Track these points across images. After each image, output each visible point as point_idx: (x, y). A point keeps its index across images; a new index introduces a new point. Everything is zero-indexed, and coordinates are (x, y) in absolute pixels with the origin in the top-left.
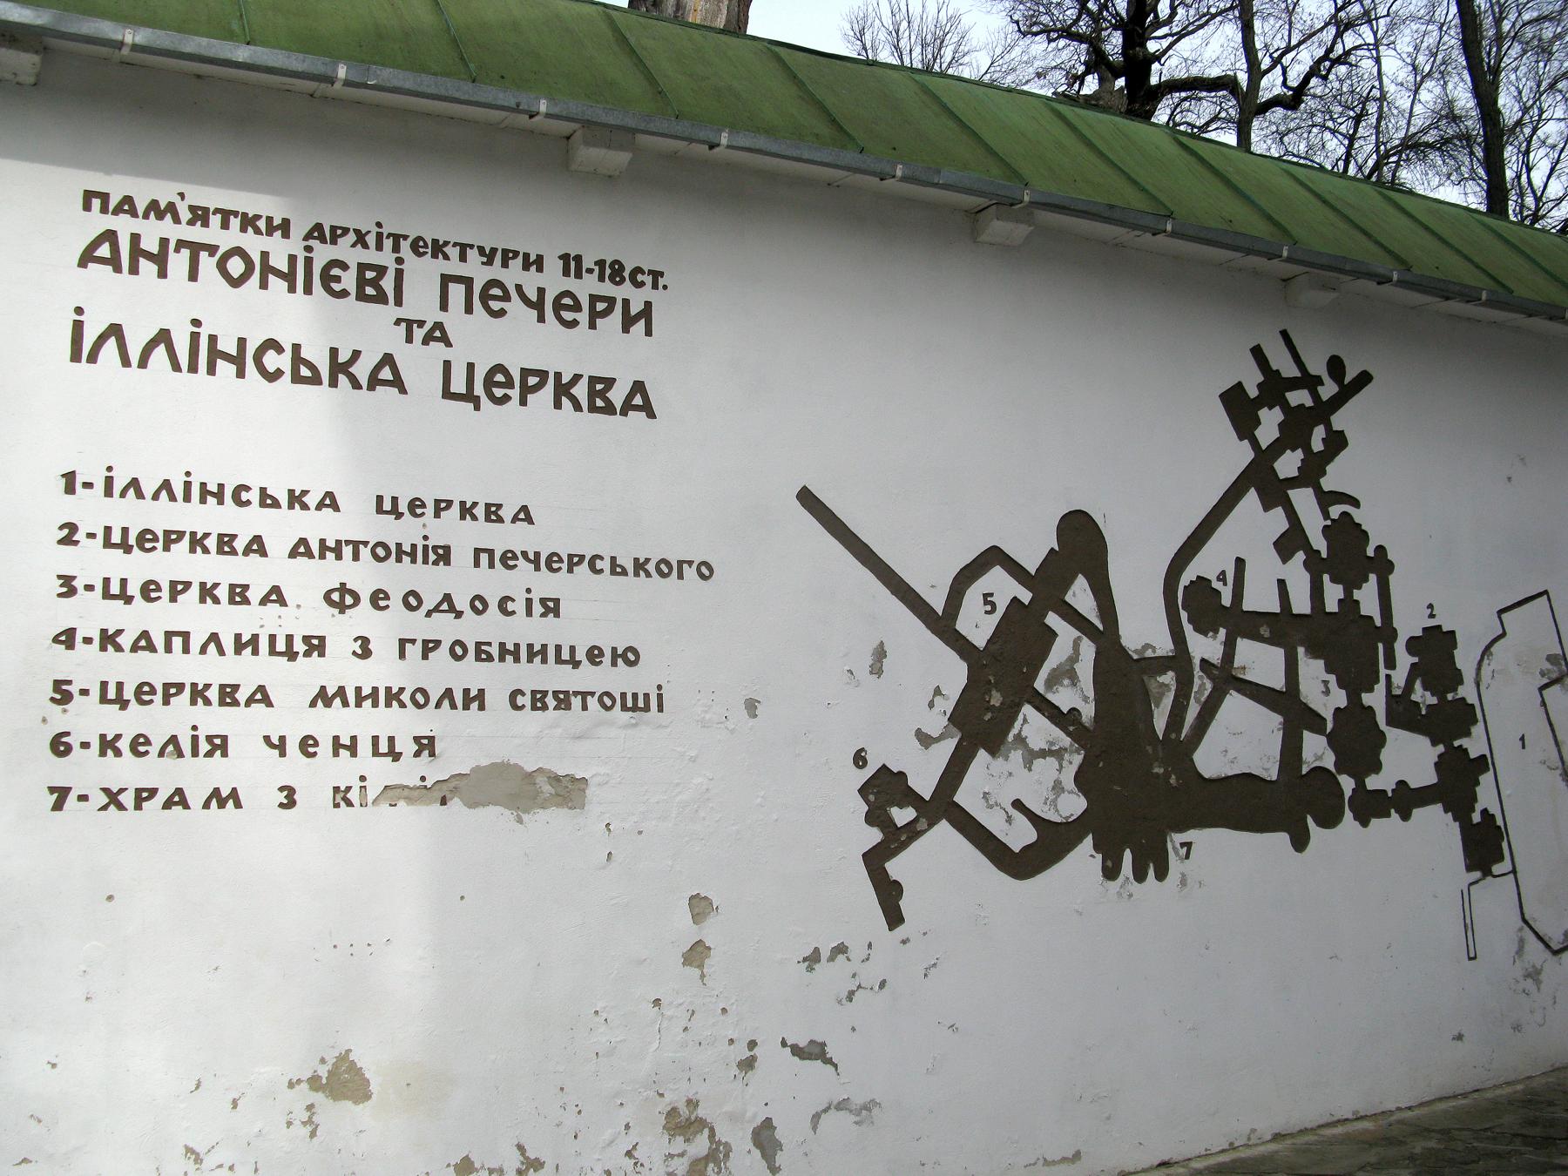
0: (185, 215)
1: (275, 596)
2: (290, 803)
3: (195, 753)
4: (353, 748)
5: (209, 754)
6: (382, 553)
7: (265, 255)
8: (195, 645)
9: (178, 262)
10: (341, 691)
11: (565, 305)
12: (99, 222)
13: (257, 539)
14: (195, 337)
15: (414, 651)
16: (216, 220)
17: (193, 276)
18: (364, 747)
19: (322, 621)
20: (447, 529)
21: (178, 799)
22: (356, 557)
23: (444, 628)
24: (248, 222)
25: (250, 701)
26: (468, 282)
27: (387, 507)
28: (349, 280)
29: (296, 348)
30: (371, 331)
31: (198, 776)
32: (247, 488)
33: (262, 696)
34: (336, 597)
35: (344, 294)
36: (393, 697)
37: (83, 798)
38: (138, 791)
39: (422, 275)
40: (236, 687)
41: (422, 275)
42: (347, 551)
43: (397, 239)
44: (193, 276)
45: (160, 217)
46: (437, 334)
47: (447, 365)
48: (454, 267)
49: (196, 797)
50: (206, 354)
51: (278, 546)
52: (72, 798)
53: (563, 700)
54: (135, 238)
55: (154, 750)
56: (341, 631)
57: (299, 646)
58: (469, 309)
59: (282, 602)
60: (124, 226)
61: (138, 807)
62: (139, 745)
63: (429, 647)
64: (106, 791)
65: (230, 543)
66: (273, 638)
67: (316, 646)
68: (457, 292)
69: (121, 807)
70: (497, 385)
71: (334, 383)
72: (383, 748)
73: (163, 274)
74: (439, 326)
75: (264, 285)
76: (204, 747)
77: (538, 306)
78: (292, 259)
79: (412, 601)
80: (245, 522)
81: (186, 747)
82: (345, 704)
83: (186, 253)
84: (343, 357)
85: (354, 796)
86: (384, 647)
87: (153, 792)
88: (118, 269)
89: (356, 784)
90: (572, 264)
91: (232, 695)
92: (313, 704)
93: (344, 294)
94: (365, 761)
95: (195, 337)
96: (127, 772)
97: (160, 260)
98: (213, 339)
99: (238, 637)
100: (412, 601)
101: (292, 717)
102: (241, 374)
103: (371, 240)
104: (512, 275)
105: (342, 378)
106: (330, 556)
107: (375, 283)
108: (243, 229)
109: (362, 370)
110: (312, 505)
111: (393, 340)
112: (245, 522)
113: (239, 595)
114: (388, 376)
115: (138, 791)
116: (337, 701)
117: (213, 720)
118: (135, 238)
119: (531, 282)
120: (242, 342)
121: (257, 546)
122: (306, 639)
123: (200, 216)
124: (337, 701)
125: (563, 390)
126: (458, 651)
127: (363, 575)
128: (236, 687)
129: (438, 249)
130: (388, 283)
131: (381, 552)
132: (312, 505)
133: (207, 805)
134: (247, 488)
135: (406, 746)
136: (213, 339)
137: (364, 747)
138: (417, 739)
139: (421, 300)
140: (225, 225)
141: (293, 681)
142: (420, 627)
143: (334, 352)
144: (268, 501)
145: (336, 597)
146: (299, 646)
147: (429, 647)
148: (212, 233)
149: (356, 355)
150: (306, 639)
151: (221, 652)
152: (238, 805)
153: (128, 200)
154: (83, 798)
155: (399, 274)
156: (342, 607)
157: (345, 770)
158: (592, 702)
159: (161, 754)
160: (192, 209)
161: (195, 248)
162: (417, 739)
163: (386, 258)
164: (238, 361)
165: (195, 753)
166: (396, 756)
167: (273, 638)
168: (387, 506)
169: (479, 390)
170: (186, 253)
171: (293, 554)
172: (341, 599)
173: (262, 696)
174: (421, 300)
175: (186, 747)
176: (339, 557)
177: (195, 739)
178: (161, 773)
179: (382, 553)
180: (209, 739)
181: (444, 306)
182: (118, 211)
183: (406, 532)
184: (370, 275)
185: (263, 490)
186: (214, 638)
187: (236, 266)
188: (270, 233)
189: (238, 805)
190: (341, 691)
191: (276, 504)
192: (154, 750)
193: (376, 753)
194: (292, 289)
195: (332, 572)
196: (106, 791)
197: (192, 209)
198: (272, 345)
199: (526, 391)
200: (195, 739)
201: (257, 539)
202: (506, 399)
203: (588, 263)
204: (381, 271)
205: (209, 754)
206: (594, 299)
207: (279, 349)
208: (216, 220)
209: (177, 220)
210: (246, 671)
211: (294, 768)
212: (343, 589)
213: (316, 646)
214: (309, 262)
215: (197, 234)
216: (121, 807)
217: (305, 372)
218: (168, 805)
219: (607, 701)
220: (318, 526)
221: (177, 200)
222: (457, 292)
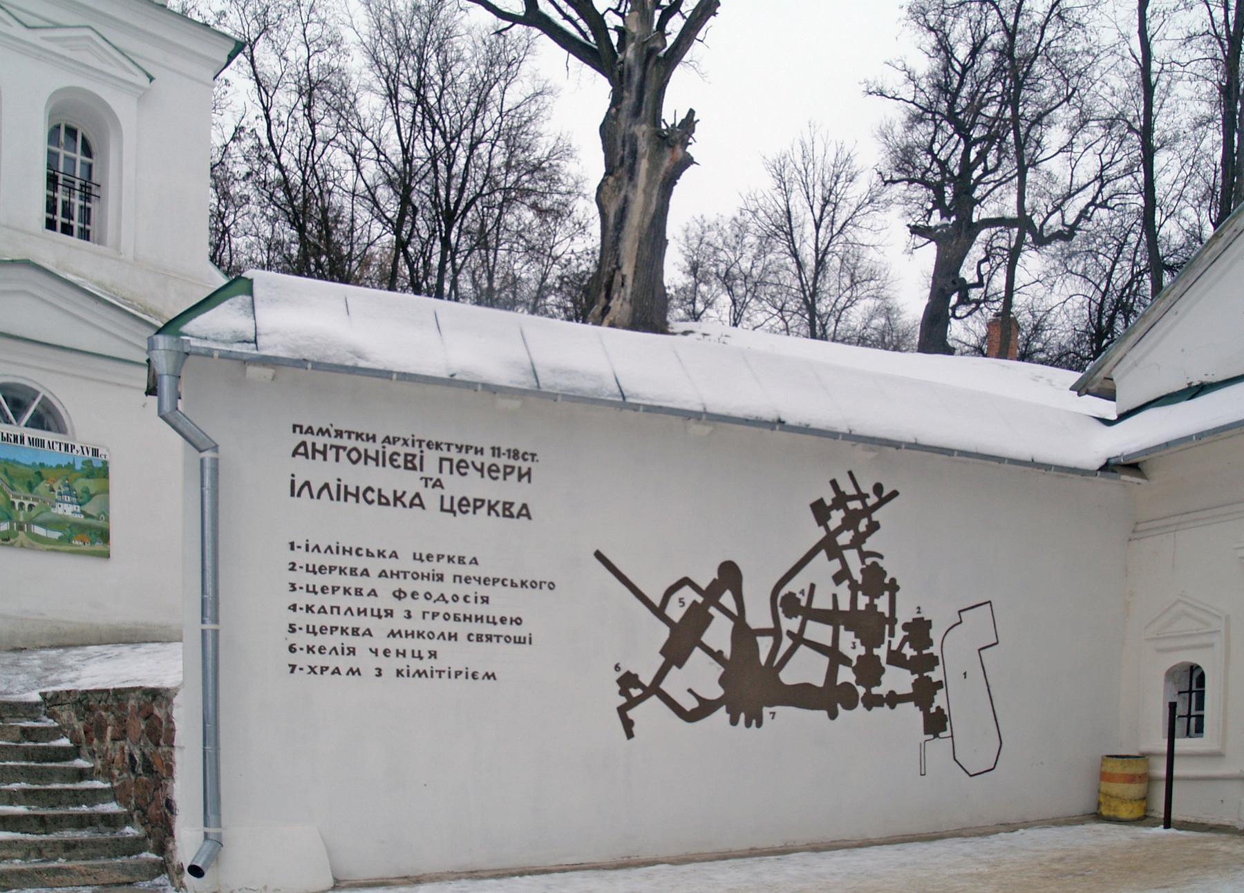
1: (373, 593)
11: (493, 469)
19: (393, 604)
20: (443, 567)
25: (364, 634)
26: (451, 460)
27: (418, 558)
28: (401, 461)
29: (380, 490)
30: (409, 482)
31: (344, 663)
33: (368, 632)
35: (399, 467)
39: (432, 457)
41: (432, 457)
42: (402, 575)
43: (421, 442)
46: (438, 484)
47: (442, 497)
48: (445, 454)
56: (399, 607)
57: (383, 613)
58: (451, 472)
59: (376, 595)
62: (321, 650)
67: (389, 613)
68: (446, 465)
70: (464, 505)
71: (395, 505)
74: (438, 480)
76: (346, 651)
77: (481, 470)
78: (377, 452)
81: (339, 651)
84: (399, 494)
90: (496, 451)
93: (399, 467)
96: (317, 660)
101: (381, 642)
103: (410, 442)
104: (470, 457)
107: (411, 462)
109: (407, 500)
111: (419, 487)
114: (417, 502)
117: (350, 641)
119: (478, 460)
125: (491, 508)
127: (408, 585)
129: (438, 446)
130: (417, 462)
139: (431, 469)
143: (395, 492)
146: (383, 613)
149: (404, 493)
155: (422, 458)
156: (400, 598)
163: (416, 450)
169: (456, 508)
172: (399, 595)
173: (368, 632)
174: (431, 469)
175: (339, 651)
178: (331, 661)
181: (441, 471)
183: (425, 568)
184: (409, 458)
195: (396, 584)
198: (370, 489)
199: (476, 508)
202: (467, 511)
203: (503, 451)
204: (414, 456)
206: (506, 467)
210: (363, 622)
212: (400, 591)
213: (389, 613)
214: (384, 453)
217: (383, 500)
220: (390, 565)
222: (446, 465)
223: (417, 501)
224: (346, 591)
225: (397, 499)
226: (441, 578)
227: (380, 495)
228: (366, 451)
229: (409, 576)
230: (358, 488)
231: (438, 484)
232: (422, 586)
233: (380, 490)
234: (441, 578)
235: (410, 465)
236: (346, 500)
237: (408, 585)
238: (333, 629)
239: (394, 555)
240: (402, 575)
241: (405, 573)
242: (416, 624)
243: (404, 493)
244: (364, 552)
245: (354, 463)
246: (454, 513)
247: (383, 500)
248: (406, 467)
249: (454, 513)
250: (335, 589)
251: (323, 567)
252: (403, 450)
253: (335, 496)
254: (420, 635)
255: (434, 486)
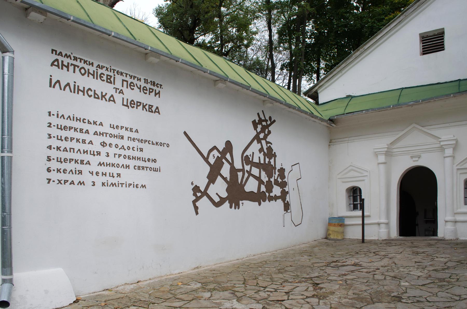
0: (73, 58)
1: (91, 143)
2: (94, 185)
3: (76, 174)
4: (106, 175)
5: (78, 174)
6: (111, 136)
7: (88, 70)
8: (76, 151)
9: (71, 68)
10: (103, 163)
12: (55, 57)
13: (87, 130)
14: (75, 85)
15: (117, 156)
16: (79, 60)
17: (74, 72)
18: (108, 175)
19: (100, 148)
21: (72, 183)
22: (106, 136)
23: (122, 152)
24: (85, 62)
25: (86, 164)
27: (112, 127)
29: (95, 91)
31: (76, 178)
32: (85, 119)
33: (88, 163)
34: (102, 144)
36: (113, 165)
37: (54, 181)
38: (65, 181)
40: (83, 161)
42: (105, 135)
44: (74, 72)
45: (67, 57)
49: (76, 183)
50: (77, 90)
51: (91, 132)
52: (51, 181)
53: (143, 168)
54: (62, 62)
55: (68, 172)
56: (103, 151)
57: (96, 153)
59: (92, 144)
60: (60, 58)
61: (65, 184)
63: (120, 156)
64: (58, 180)
65: (82, 131)
66: (90, 151)
67: (99, 153)
69: (61, 184)
71: (102, 99)
72: (111, 175)
73: (68, 70)
75: (88, 76)
76: (77, 172)
78: (94, 71)
79: (117, 146)
80: (85, 127)
81: (74, 172)
82: (104, 166)
83: (73, 66)
84: (104, 94)
85: (106, 184)
86: (111, 155)
87: (68, 181)
88: (59, 68)
89: (106, 182)
91: (83, 162)
92: (98, 165)
94: (108, 178)
95: (75, 85)
96: (62, 177)
97: (67, 67)
98: (78, 86)
99: (84, 150)
100: (117, 146)
101: (95, 168)
102: (84, 95)
105: (103, 98)
106: (101, 135)
108: (84, 63)
109: (107, 97)
110: (98, 124)
112: (85, 127)
113: (84, 142)
115: (65, 181)
116: (103, 165)
117: (79, 167)
118: (62, 62)
120: (84, 88)
121: (87, 132)
122: (97, 152)
123: (76, 59)
124: (103, 165)
126: (125, 157)
127: (108, 140)
128: (83, 161)
131: (111, 136)
132: (98, 124)
133: (78, 184)
134: (85, 119)
135: (115, 175)
136: (78, 86)
137: (108, 175)
138: (117, 174)
140: (81, 62)
141: (95, 160)
142: (118, 151)
143: (102, 93)
144: (89, 122)
145: (102, 144)
146: (96, 153)
147: (120, 156)
148: (77, 63)
150: (97, 152)
151: (81, 153)
152: (84, 185)
153: (61, 53)
154: (54, 181)
156: (104, 146)
157: (104, 179)
158: (148, 169)
159: (69, 173)
160: (74, 57)
161: (75, 66)
162: (117, 174)
164: (83, 92)
165: (76, 174)
166: (114, 177)
167: (90, 151)
168: (112, 126)
170: (73, 66)
171: (94, 134)
172: (103, 144)
173: (88, 163)
175: (74, 172)
176: (103, 136)
177: (76, 170)
178: (70, 177)
179: (111, 136)
180: (78, 171)
182: (59, 55)
183: (115, 132)
185: (88, 120)
186: (79, 150)
187: (83, 71)
188: (89, 65)
189: (84, 185)
190: (103, 163)
191: (91, 123)
192: (68, 172)
193: (110, 176)
194: (94, 78)
196: (58, 180)
197: (74, 57)
198: (90, 89)
200: (76, 170)
201: (87, 130)
205: (78, 174)
207: (91, 91)
208: (79, 60)
209: (71, 59)
210: (86, 157)
211: (95, 178)
212: (104, 142)
213: (99, 153)
215: (75, 63)
216: (61, 184)
217: (96, 96)
218: (71, 184)
219: (151, 169)
220: (99, 129)
221: (71, 54)
223: (112, 99)
224: (78, 140)
225: (103, 96)
226: (122, 138)
227: (95, 93)
228: (88, 70)
229: (108, 135)
230: (84, 88)
231: (121, 92)
232: (114, 141)
233: (95, 91)
234: (122, 138)
235: (109, 81)
236: (78, 93)
237: (108, 140)
238: (71, 160)
239: (101, 124)
240: (105, 135)
241: (106, 133)
242: (111, 160)
243: (106, 94)
244: (86, 121)
245: (83, 75)
246: (128, 107)
247: (96, 96)
248: (107, 82)
249: (128, 107)
250: (72, 139)
251: (66, 127)
252: (106, 73)
253: (73, 90)
254: (113, 165)
255: (120, 92)
